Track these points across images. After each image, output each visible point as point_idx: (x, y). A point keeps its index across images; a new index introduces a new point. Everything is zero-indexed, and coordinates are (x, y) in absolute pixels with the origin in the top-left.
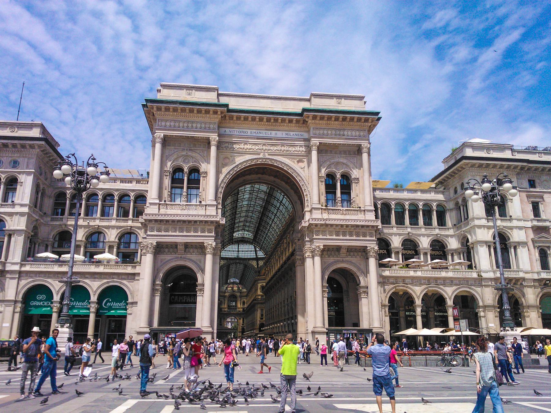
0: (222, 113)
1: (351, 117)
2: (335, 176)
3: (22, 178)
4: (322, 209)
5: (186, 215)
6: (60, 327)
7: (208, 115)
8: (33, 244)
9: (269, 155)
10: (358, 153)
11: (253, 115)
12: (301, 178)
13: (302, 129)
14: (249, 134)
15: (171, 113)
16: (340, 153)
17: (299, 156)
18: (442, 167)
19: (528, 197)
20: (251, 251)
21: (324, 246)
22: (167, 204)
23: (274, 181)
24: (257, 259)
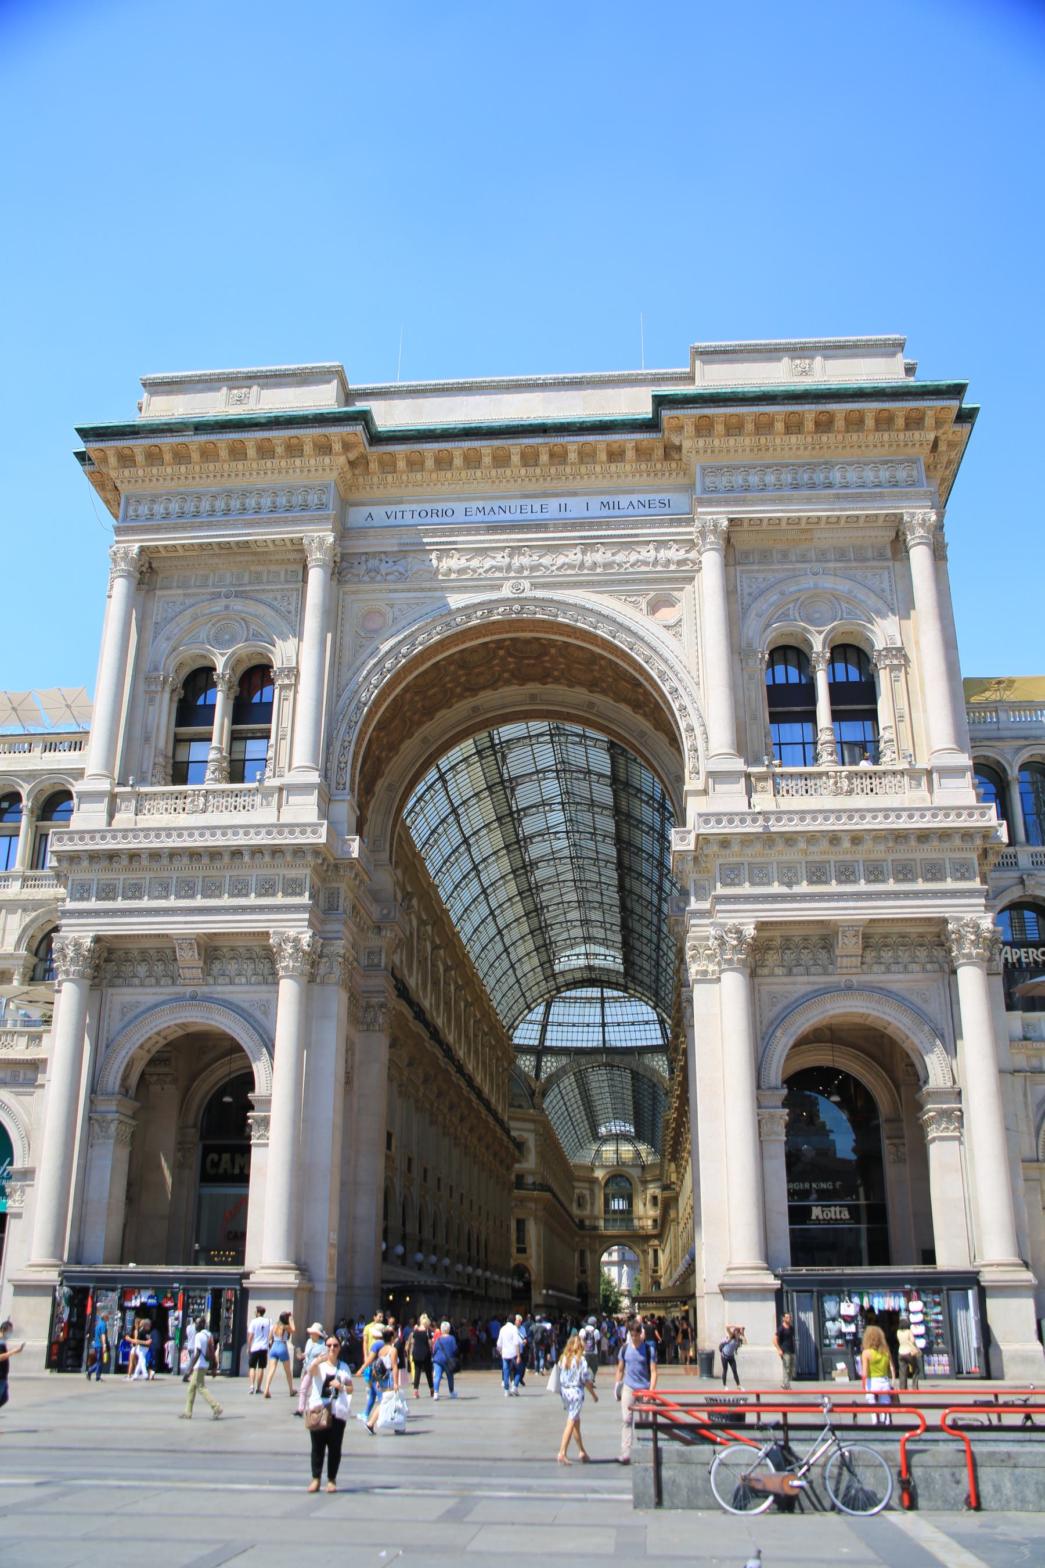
0: (347, 447)
2: (806, 650)
4: (748, 776)
5: (202, 830)
7: (298, 462)
9: (534, 586)
11: (467, 444)
12: (666, 661)
14: (460, 516)
15: (169, 470)
16: (822, 556)
17: (655, 581)
20: (647, 1023)
21: (761, 926)
23: (592, 705)
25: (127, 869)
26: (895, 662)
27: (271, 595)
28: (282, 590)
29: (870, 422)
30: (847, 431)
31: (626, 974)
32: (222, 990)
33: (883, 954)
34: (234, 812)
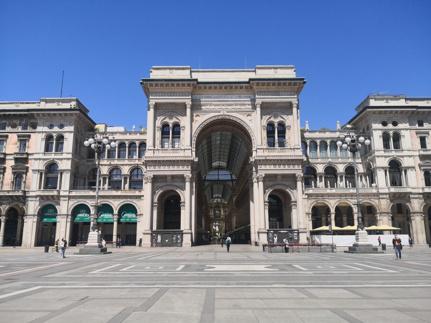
1: (284, 82)
3: (66, 135)
4: (264, 149)
5: (172, 157)
6: (92, 231)
7: (184, 87)
8: (76, 178)
9: (227, 112)
10: (290, 108)
11: (215, 85)
12: (249, 127)
13: (250, 93)
16: (277, 108)
18: (355, 113)
19: (417, 133)
20: (228, 175)
21: (265, 174)
22: (159, 150)
24: (232, 180)
25: (158, 163)
26: (289, 128)
27: (179, 112)
28: (181, 111)
29: (287, 84)
30: (283, 86)
31: (227, 167)
32: (174, 184)
33: (285, 179)
34: (175, 153)
